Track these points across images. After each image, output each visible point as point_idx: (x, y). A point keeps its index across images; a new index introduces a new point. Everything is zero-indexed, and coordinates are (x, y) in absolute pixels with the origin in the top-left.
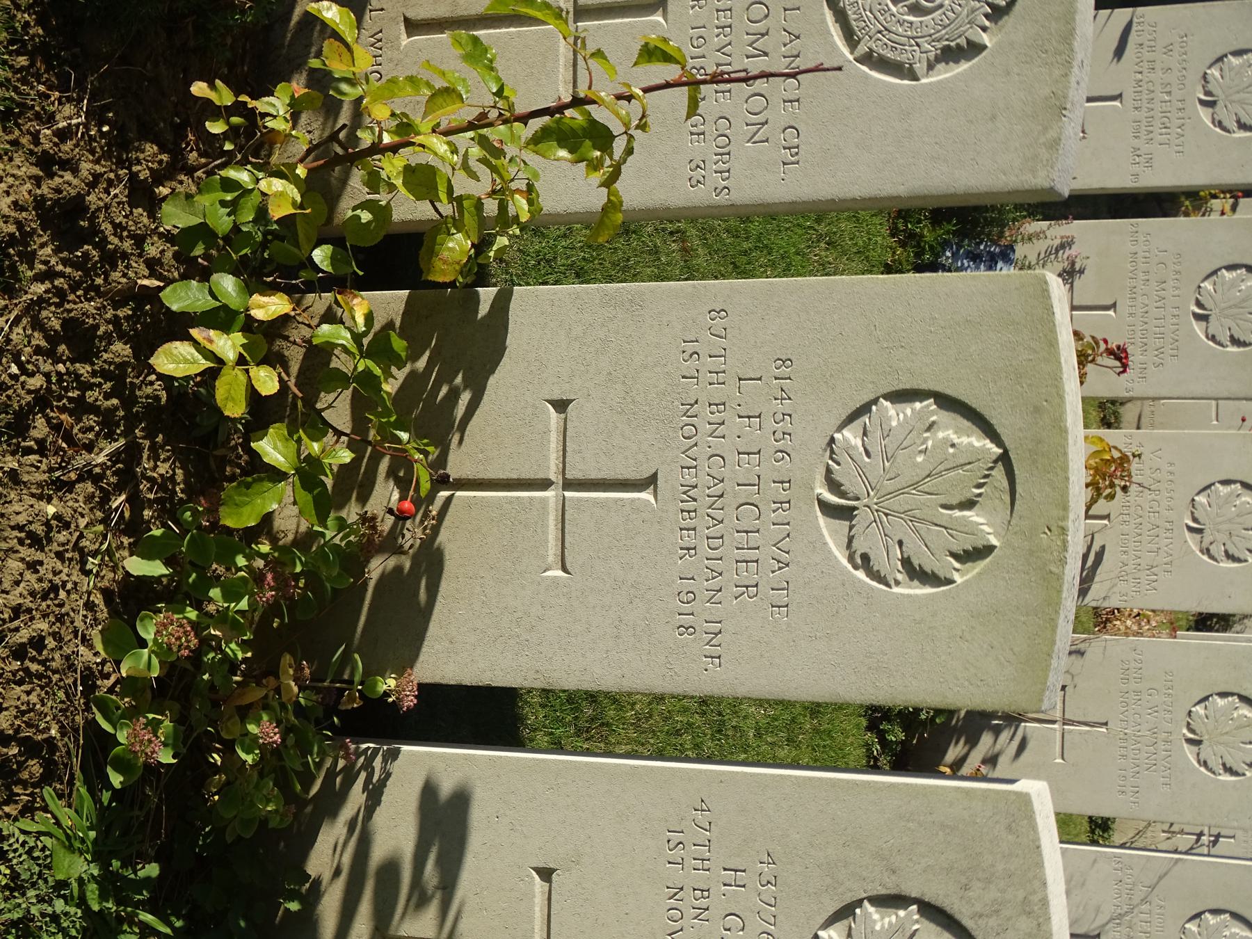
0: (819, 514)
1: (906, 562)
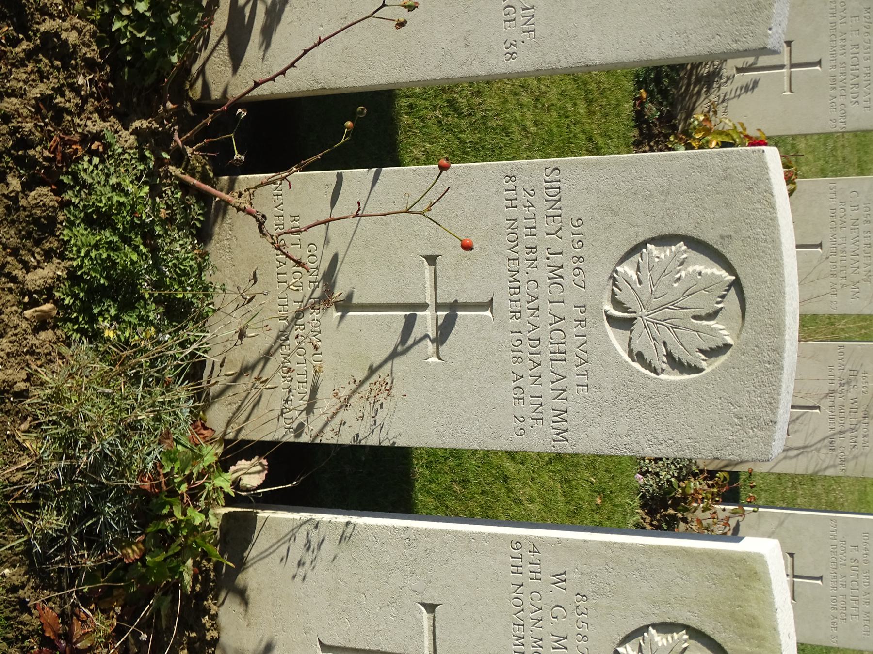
0: (607, 324)
1: (669, 355)
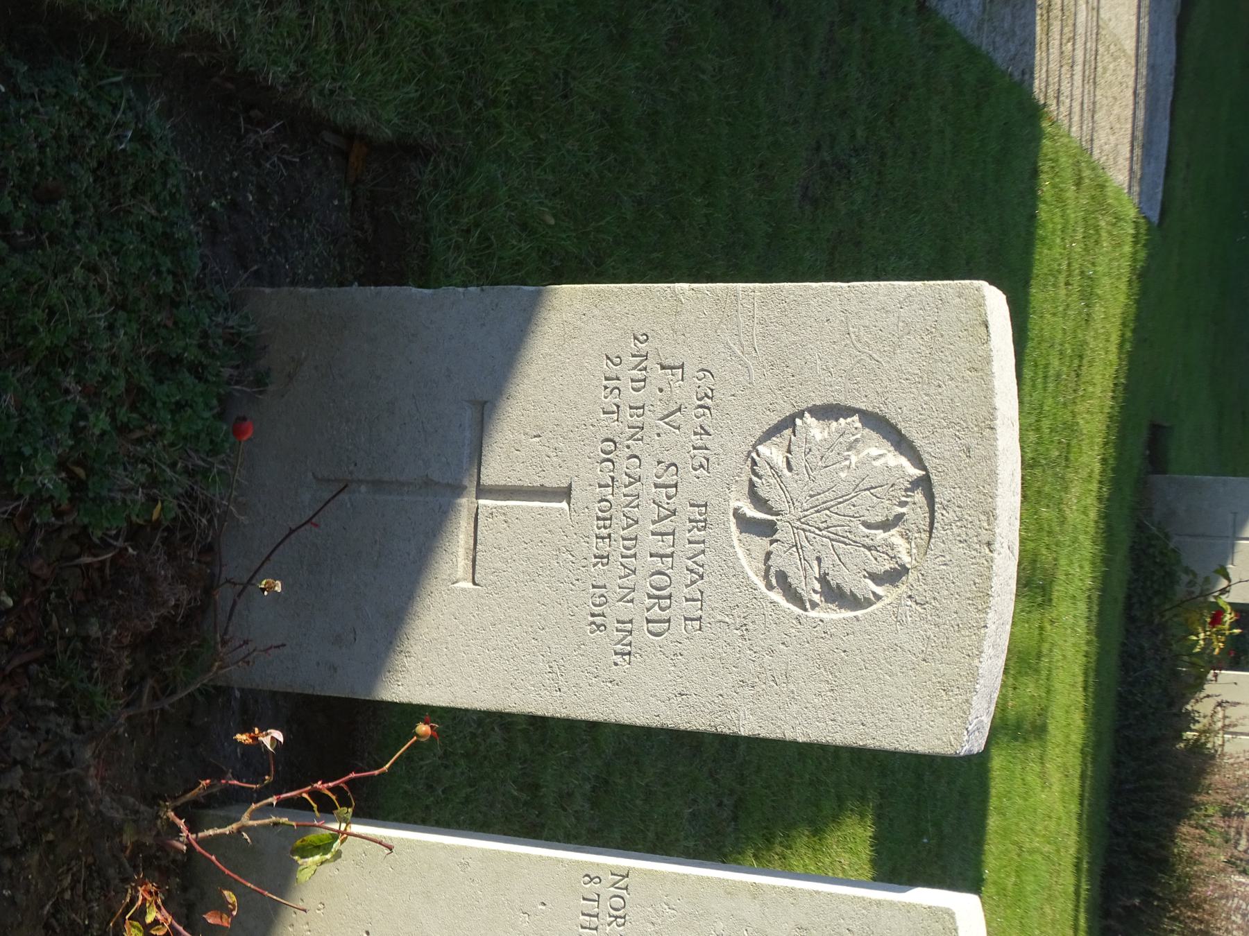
1: (823, 579)
